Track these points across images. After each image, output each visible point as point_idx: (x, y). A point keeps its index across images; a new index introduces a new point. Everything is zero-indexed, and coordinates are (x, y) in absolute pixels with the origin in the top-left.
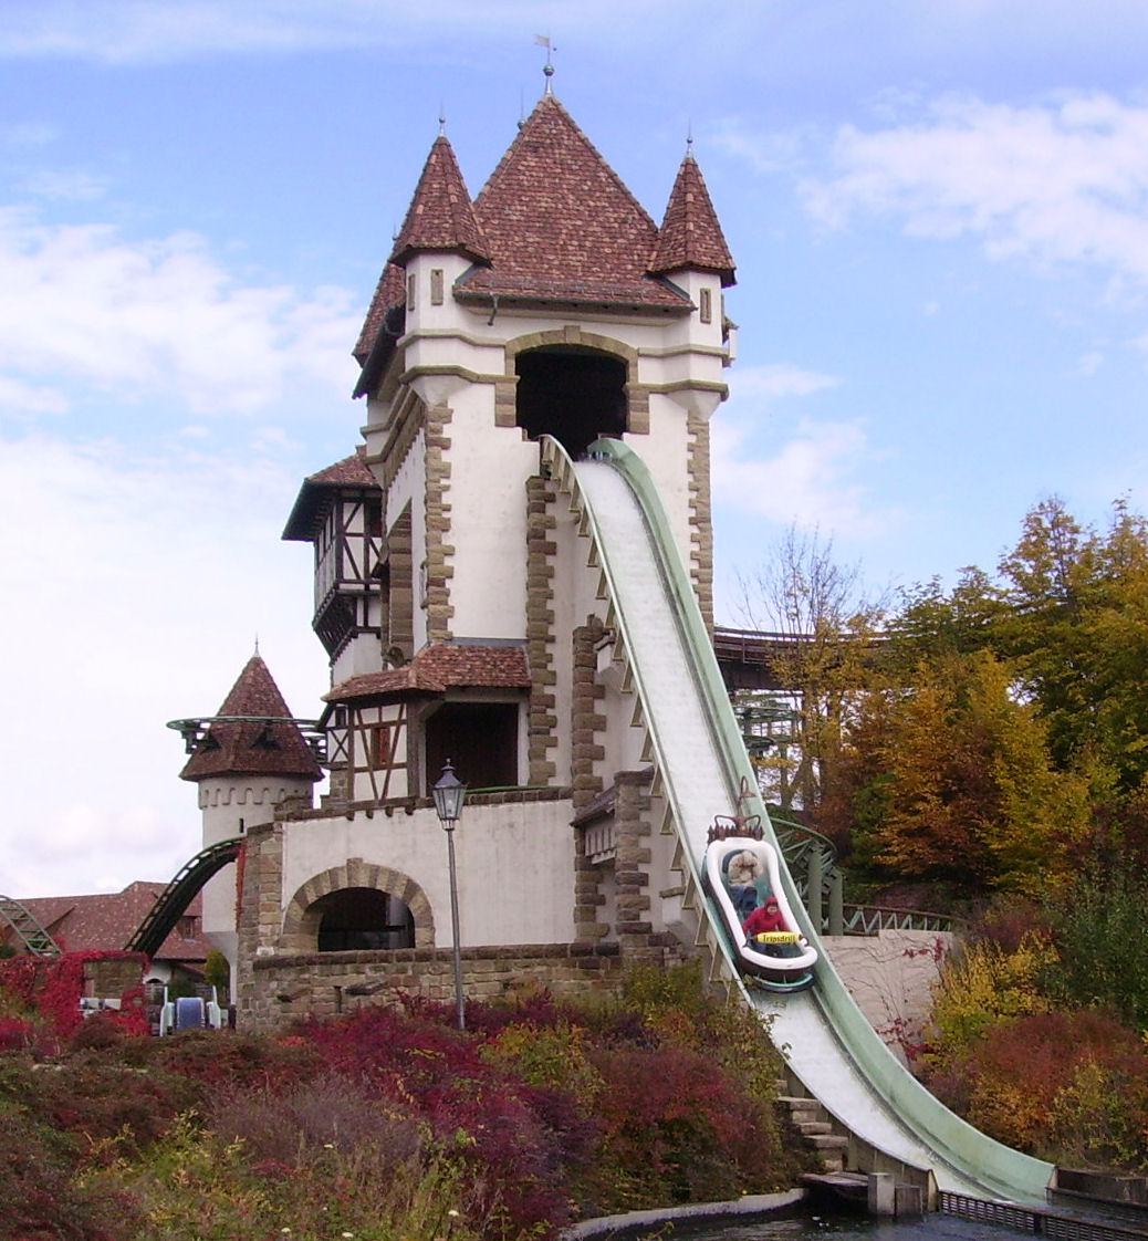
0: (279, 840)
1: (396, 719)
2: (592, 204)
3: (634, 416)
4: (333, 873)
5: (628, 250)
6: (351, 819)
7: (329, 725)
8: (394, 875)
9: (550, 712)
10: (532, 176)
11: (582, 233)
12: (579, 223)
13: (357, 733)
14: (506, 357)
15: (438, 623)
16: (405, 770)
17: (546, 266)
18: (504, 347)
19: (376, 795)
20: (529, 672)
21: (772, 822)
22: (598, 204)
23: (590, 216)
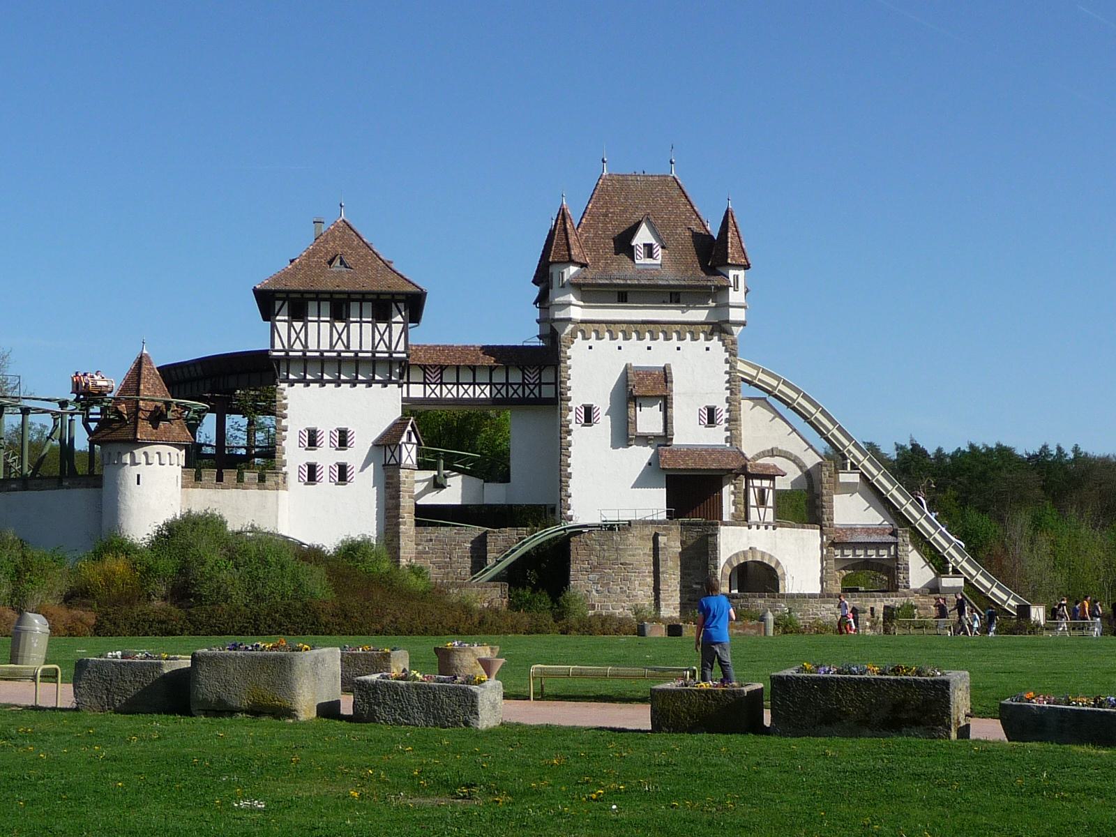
1: (768, 486)
8: (771, 557)
13: (752, 489)
19: (760, 519)
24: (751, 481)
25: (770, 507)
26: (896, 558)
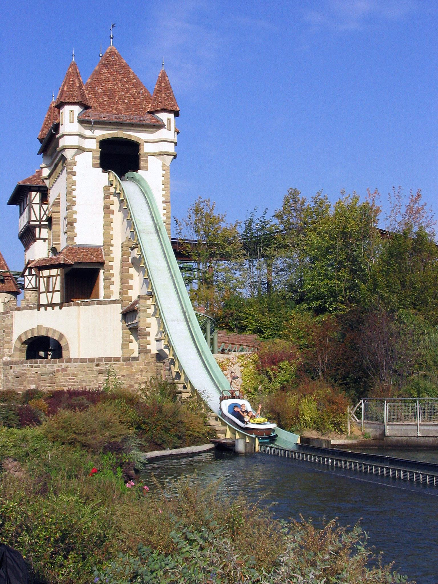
0: (12, 317)
1: (56, 274)
2: (127, 86)
3: (142, 164)
4: (32, 330)
5: (141, 103)
6: (39, 310)
7: (25, 274)
9: (111, 272)
10: (105, 76)
11: (124, 97)
12: (123, 93)
13: (41, 279)
14: (97, 142)
15: (71, 239)
16: (59, 293)
17: (111, 109)
18: (95, 138)
20: (104, 256)
21: (197, 315)
22: (130, 86)
23: (127, 90)
24: (41, 272)
25: (58, 291)
26: (137, 326)
